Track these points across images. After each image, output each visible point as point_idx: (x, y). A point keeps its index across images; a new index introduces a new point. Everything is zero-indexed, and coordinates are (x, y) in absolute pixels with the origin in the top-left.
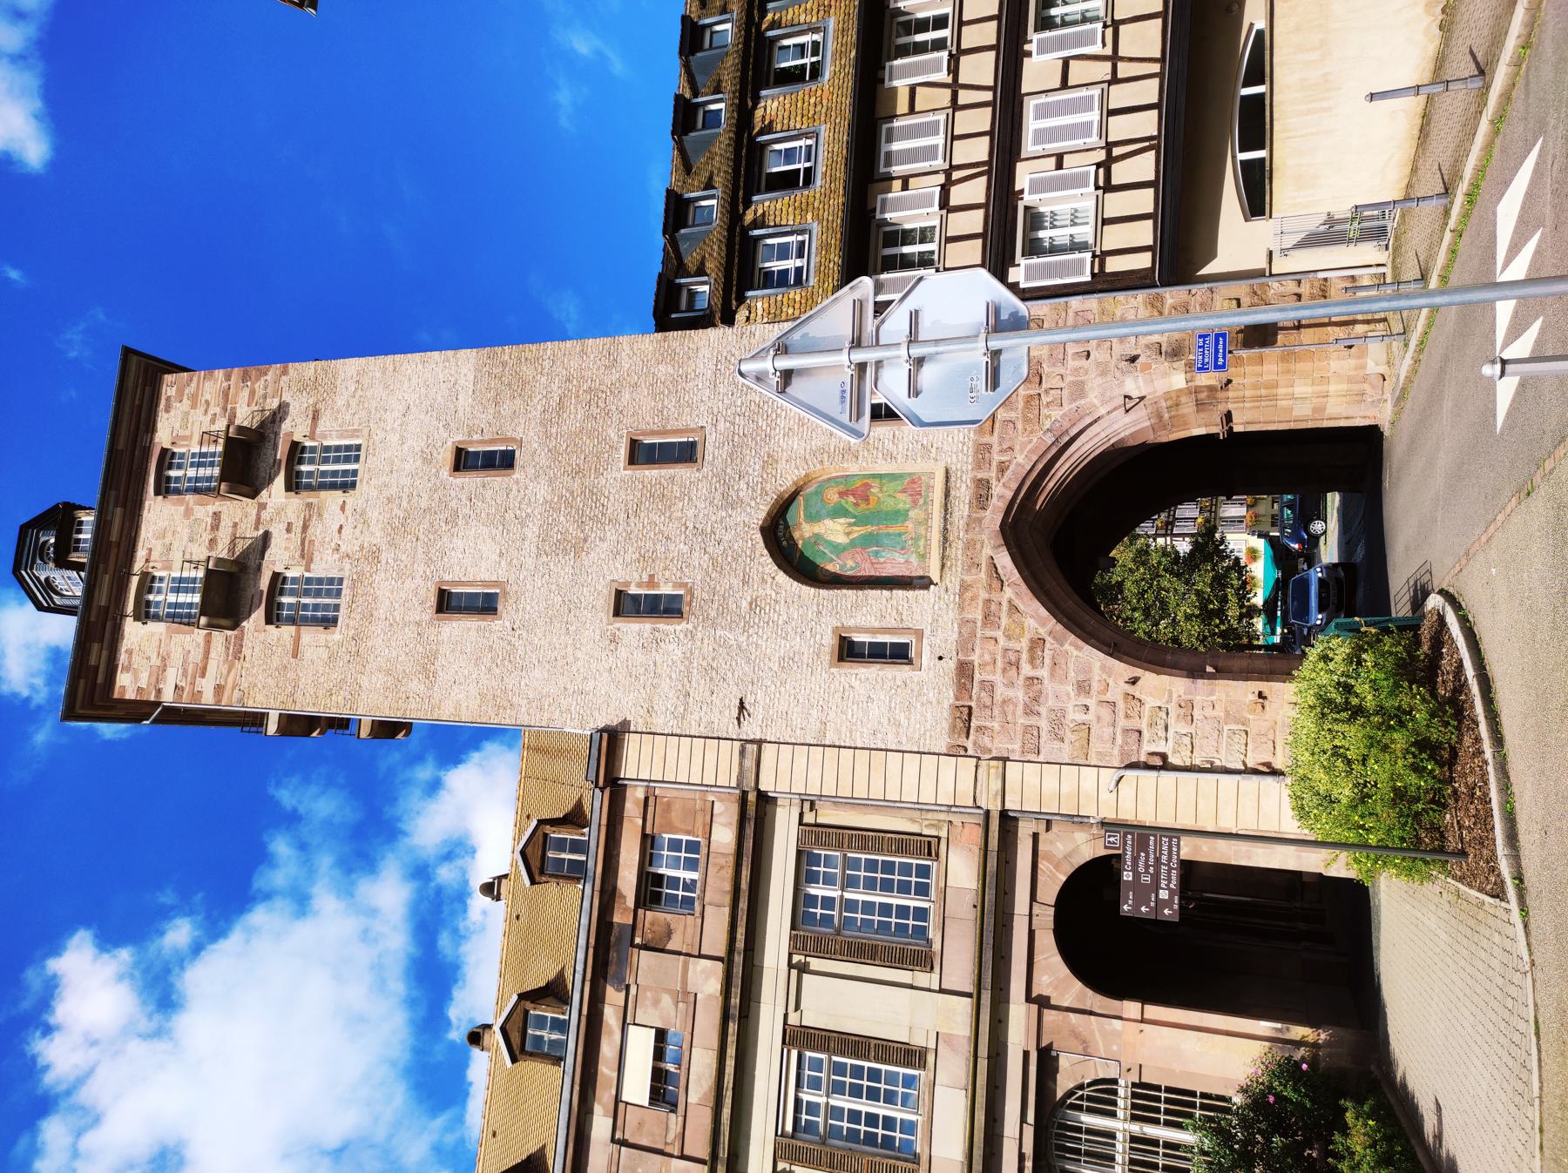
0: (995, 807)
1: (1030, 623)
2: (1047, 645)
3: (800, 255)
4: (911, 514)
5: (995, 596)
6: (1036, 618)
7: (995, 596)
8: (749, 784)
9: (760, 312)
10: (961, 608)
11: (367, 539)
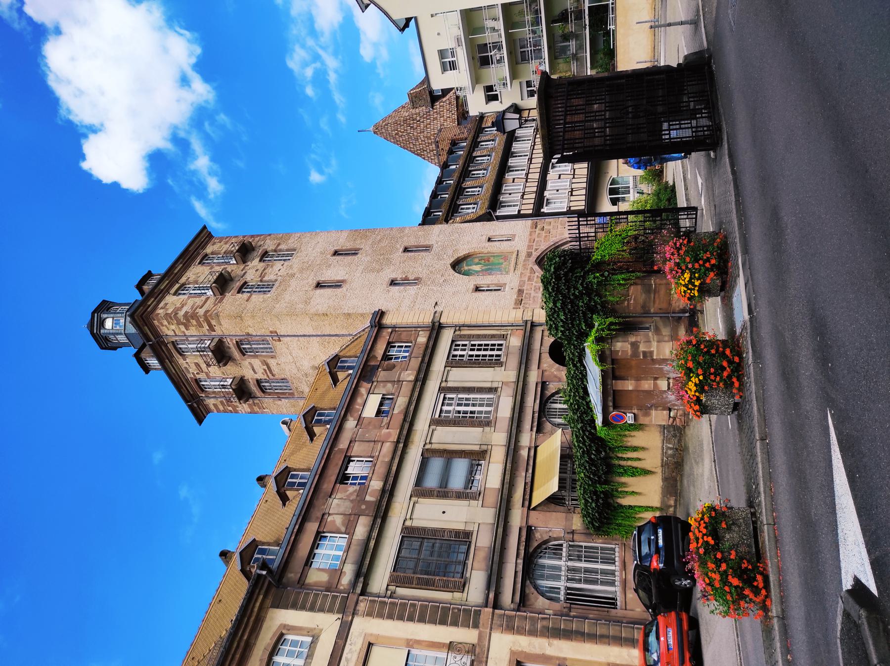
8: (437, 319)
11: (291, 271)
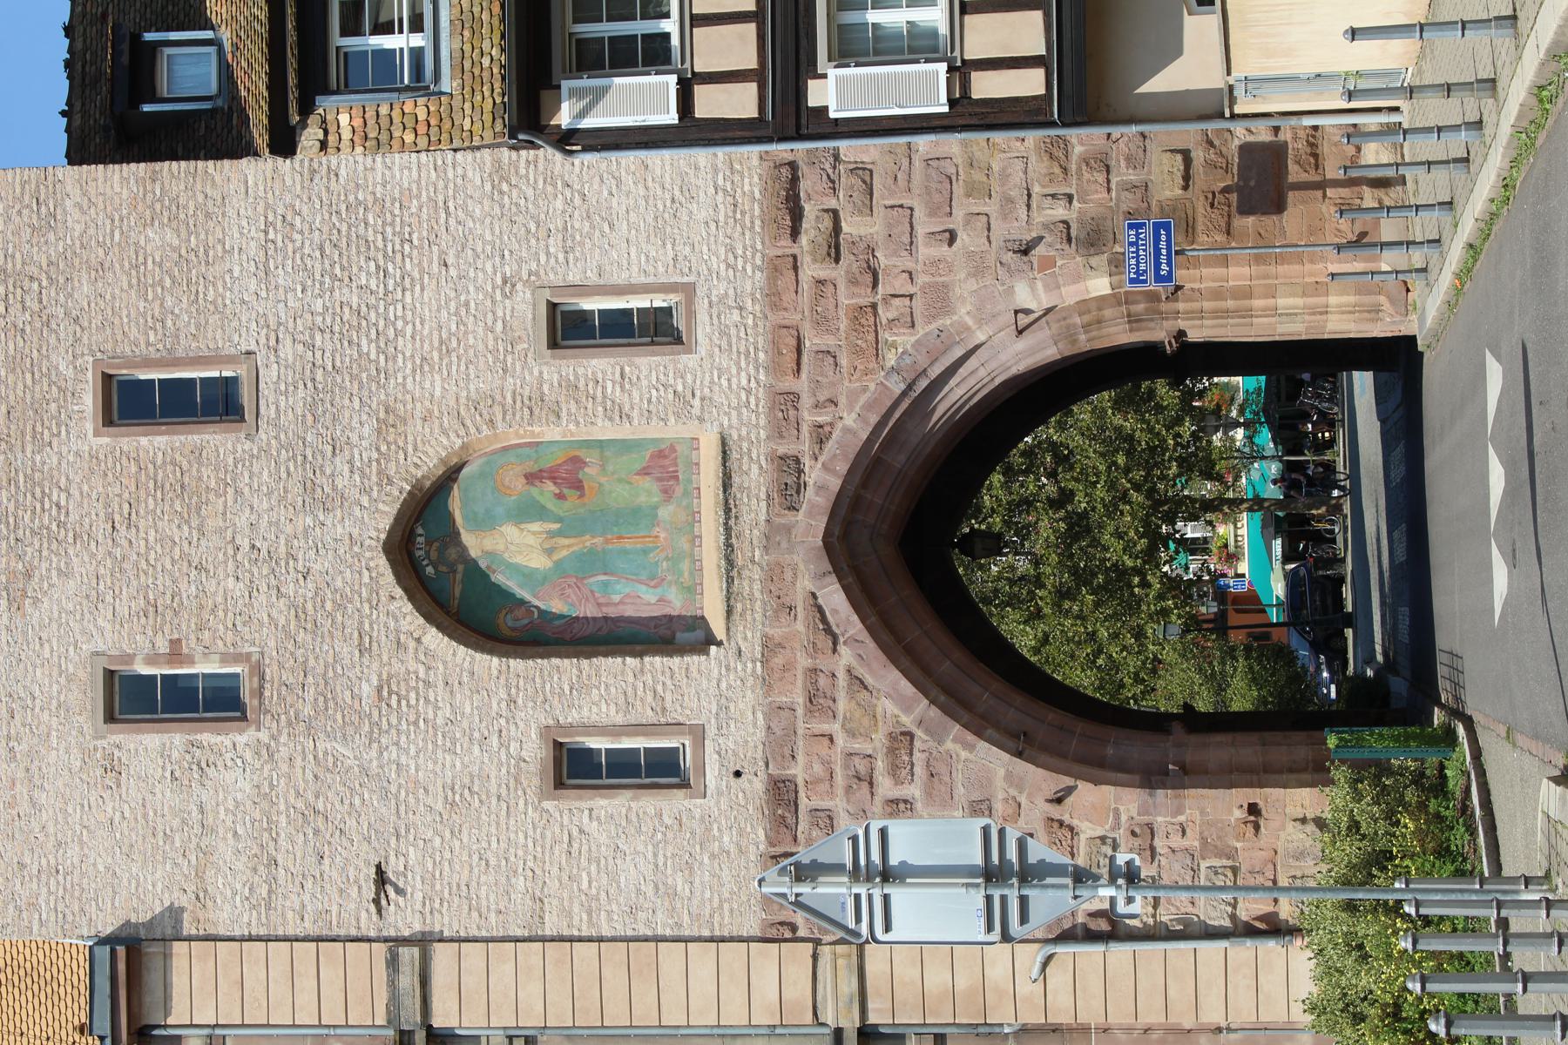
0: (850, 1023)
1: (887, 706)
2: (917, 744)
3: (417, 25)
4: (665, 513)
5: (824, 662)
6: (895, 699)
7: (824, 662)
8: (411, 1017)
9: (346, 134)
10: (767, 684)
